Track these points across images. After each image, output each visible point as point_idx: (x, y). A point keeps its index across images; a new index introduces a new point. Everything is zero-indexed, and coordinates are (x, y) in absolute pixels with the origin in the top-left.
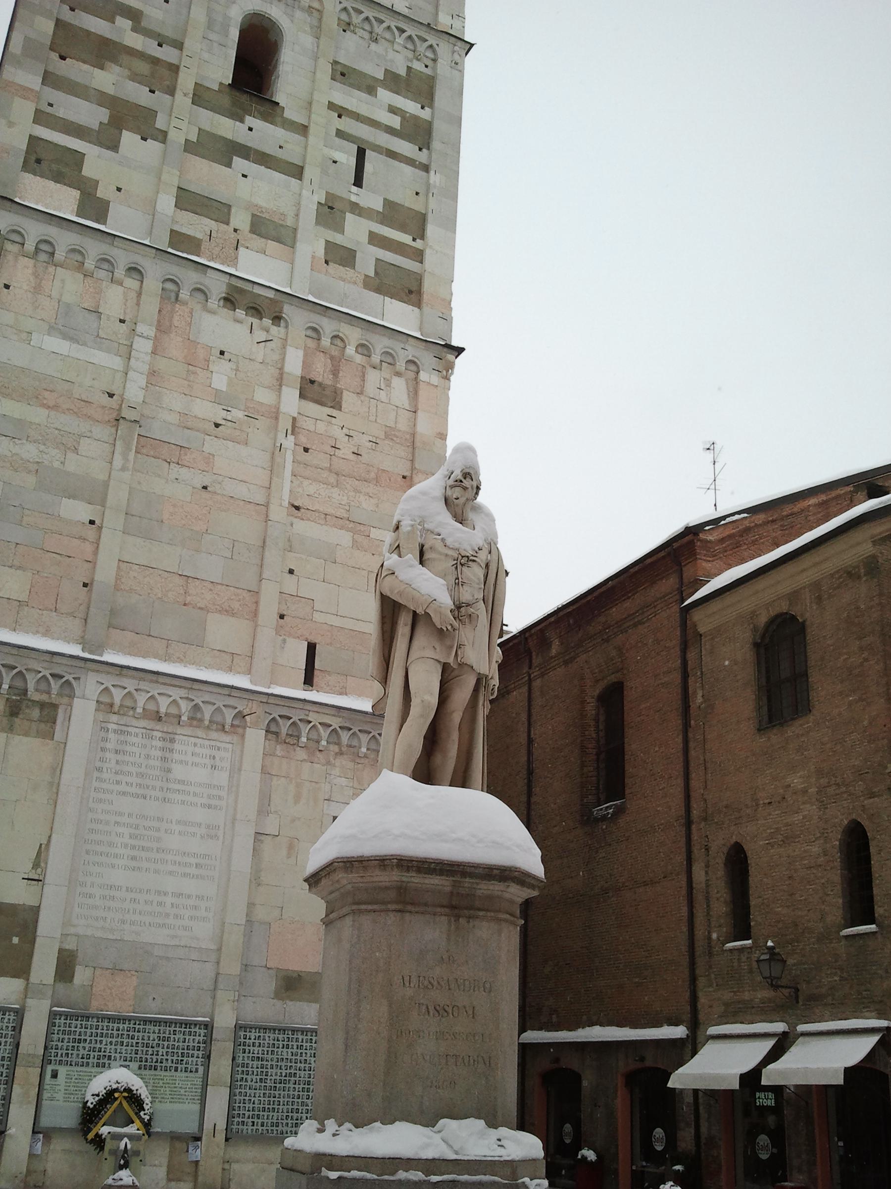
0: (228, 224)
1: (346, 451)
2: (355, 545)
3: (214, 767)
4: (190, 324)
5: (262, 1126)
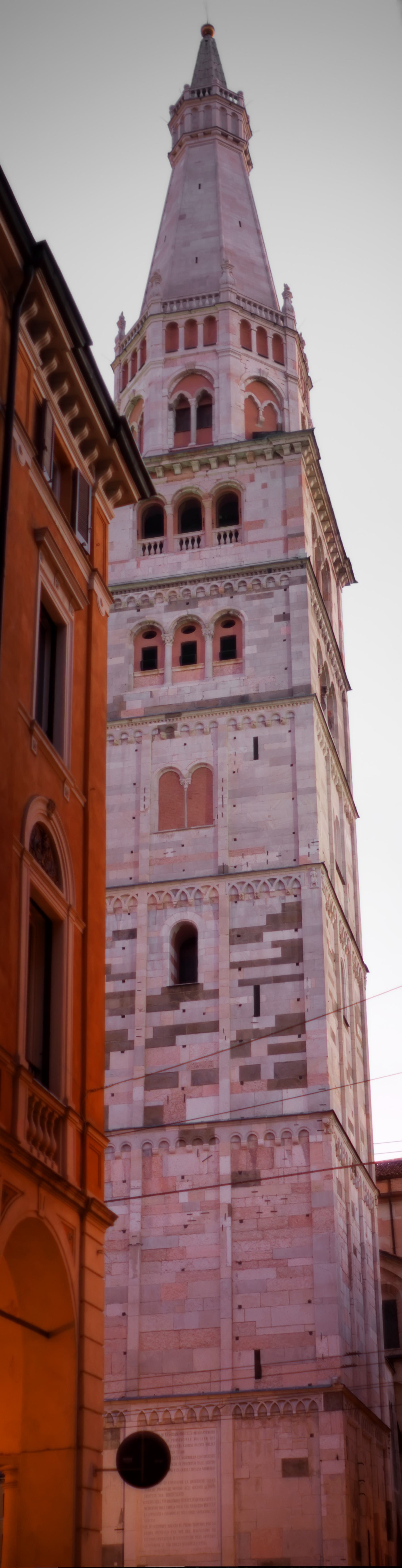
1: (267, 1213)
2: (280, 1275)
3: (207, 1444)
4: (162, 1167)
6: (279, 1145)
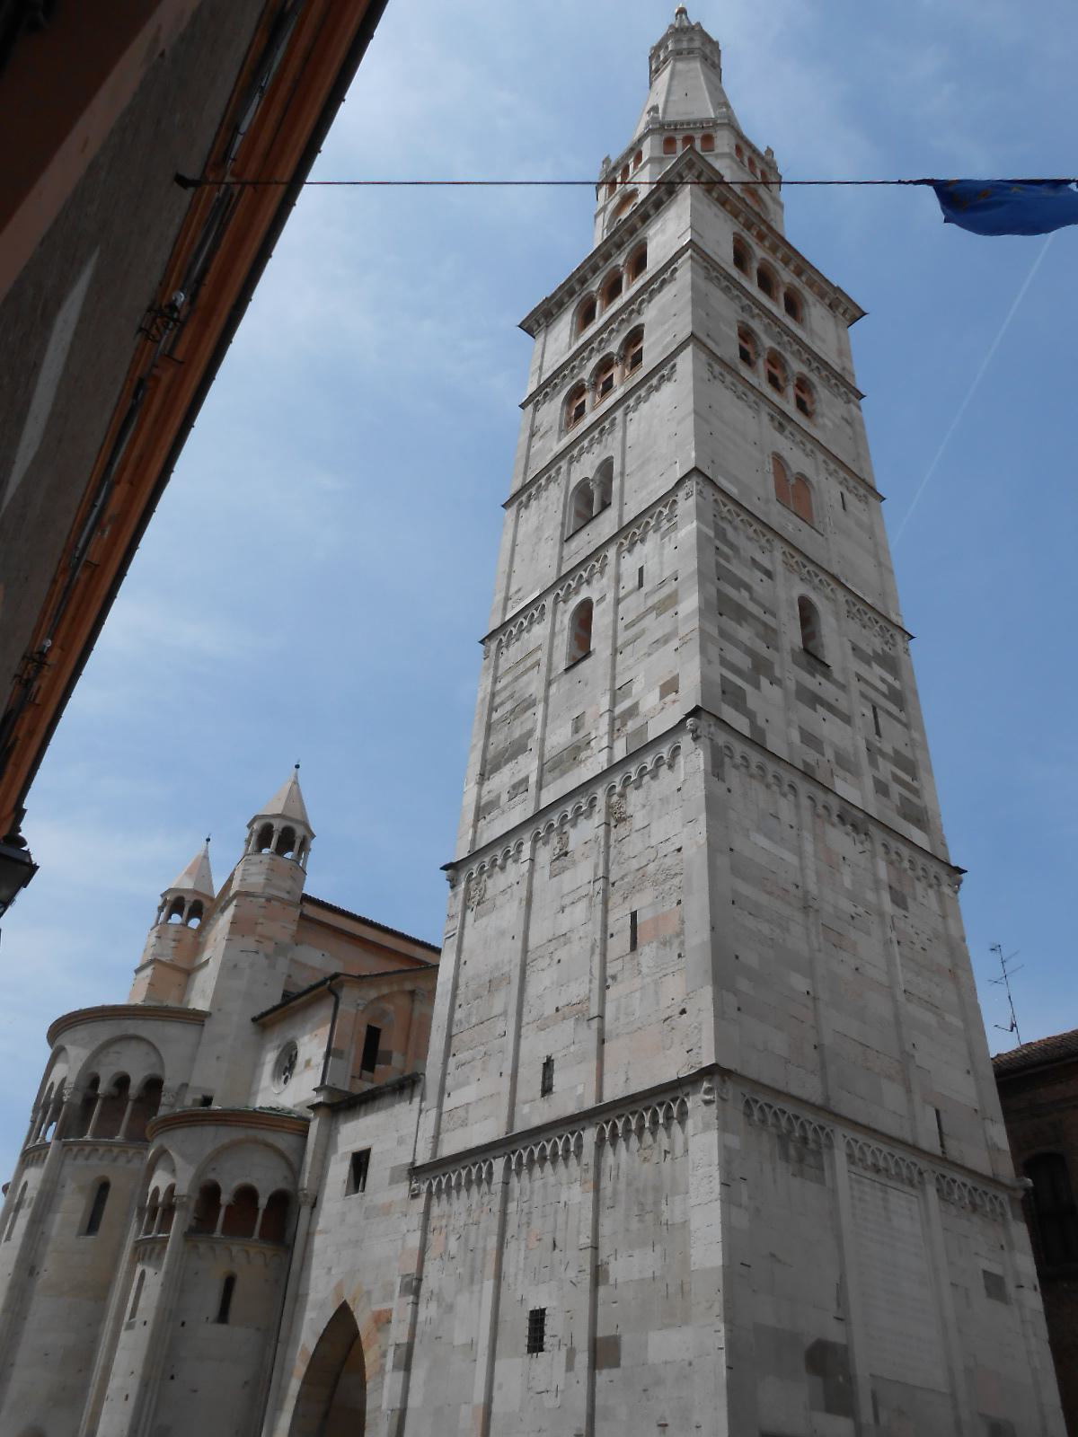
0: (823, 755)
1: (918, 947)
6: (918, 879)
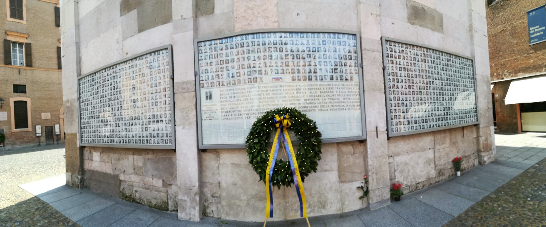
5: (416, 123)
